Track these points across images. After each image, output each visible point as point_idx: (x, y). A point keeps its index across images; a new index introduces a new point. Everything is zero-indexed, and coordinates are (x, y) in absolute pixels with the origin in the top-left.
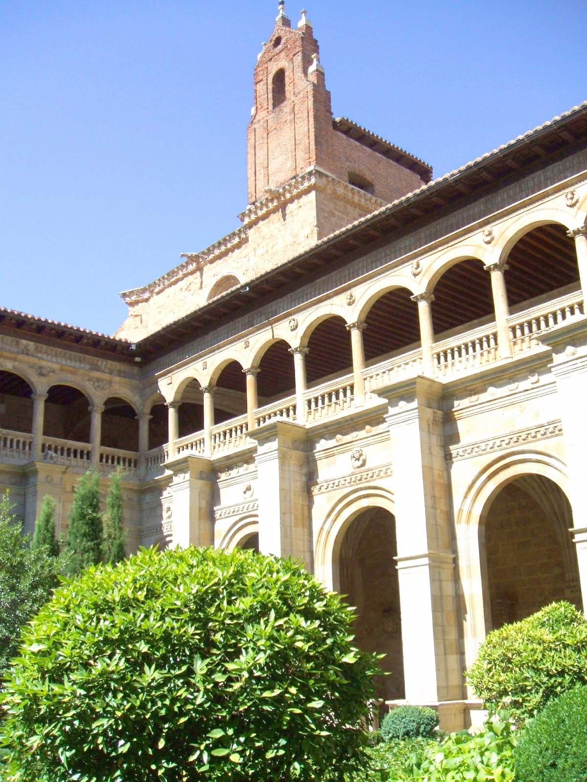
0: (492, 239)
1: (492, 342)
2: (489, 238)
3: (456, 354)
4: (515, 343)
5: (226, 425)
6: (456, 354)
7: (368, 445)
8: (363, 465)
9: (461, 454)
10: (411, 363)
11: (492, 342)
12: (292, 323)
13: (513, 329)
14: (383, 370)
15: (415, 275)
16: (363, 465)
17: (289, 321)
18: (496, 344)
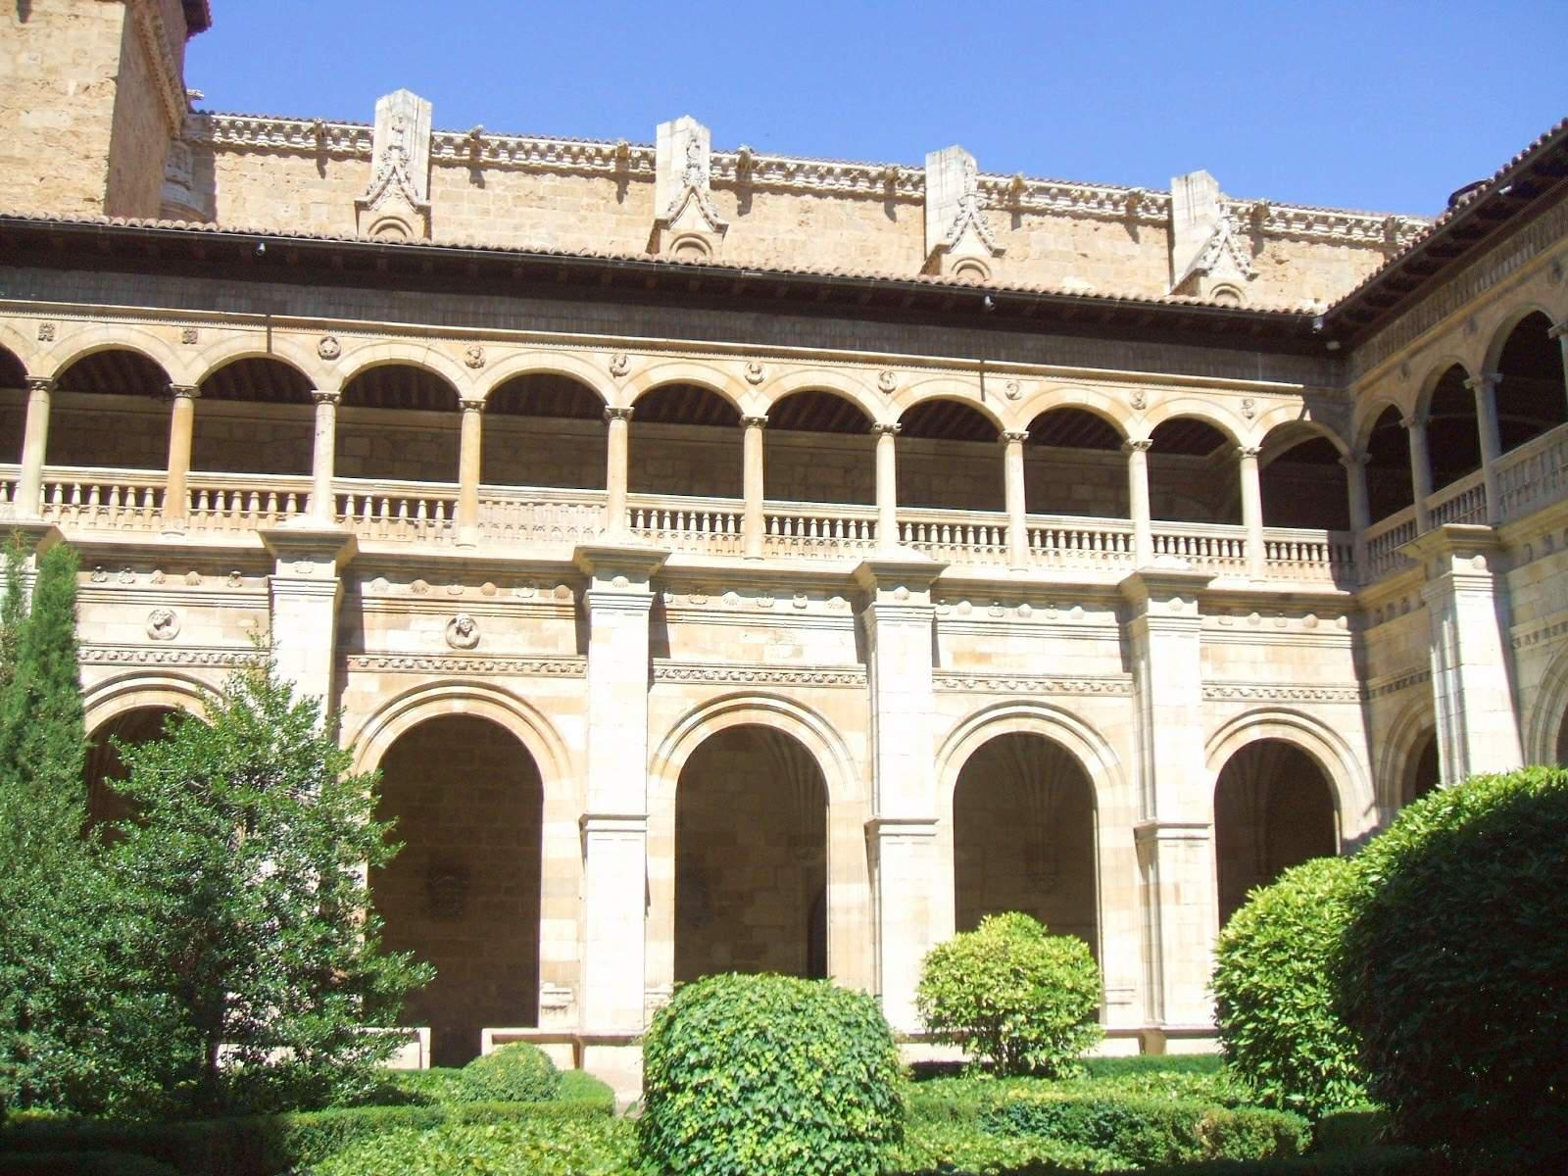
0: (761, 381)
1: (731, 526)
2: (756, 377)
3: (667, 522)
4: (768, 540)
5: (95, 475)
6: (667, 522)
7: (487, 615)
8: (474, 645)
9: (672, 674)
10: (581, 507)
11: (731, 526)
12: (329, 346)
13: (769, 520)
14: (525, 500)
15: (616, 374)
16: (474, 645)
17: (320, 338)
18: (737, 530)
